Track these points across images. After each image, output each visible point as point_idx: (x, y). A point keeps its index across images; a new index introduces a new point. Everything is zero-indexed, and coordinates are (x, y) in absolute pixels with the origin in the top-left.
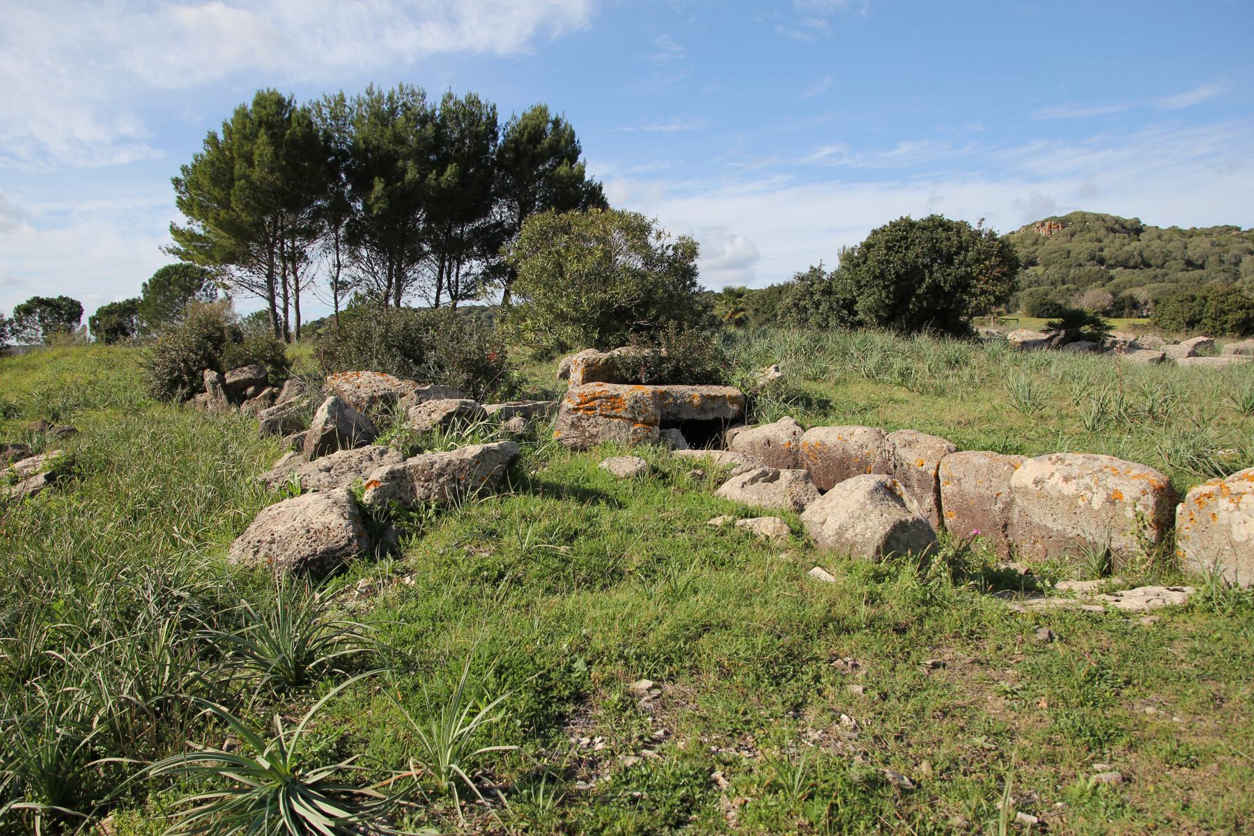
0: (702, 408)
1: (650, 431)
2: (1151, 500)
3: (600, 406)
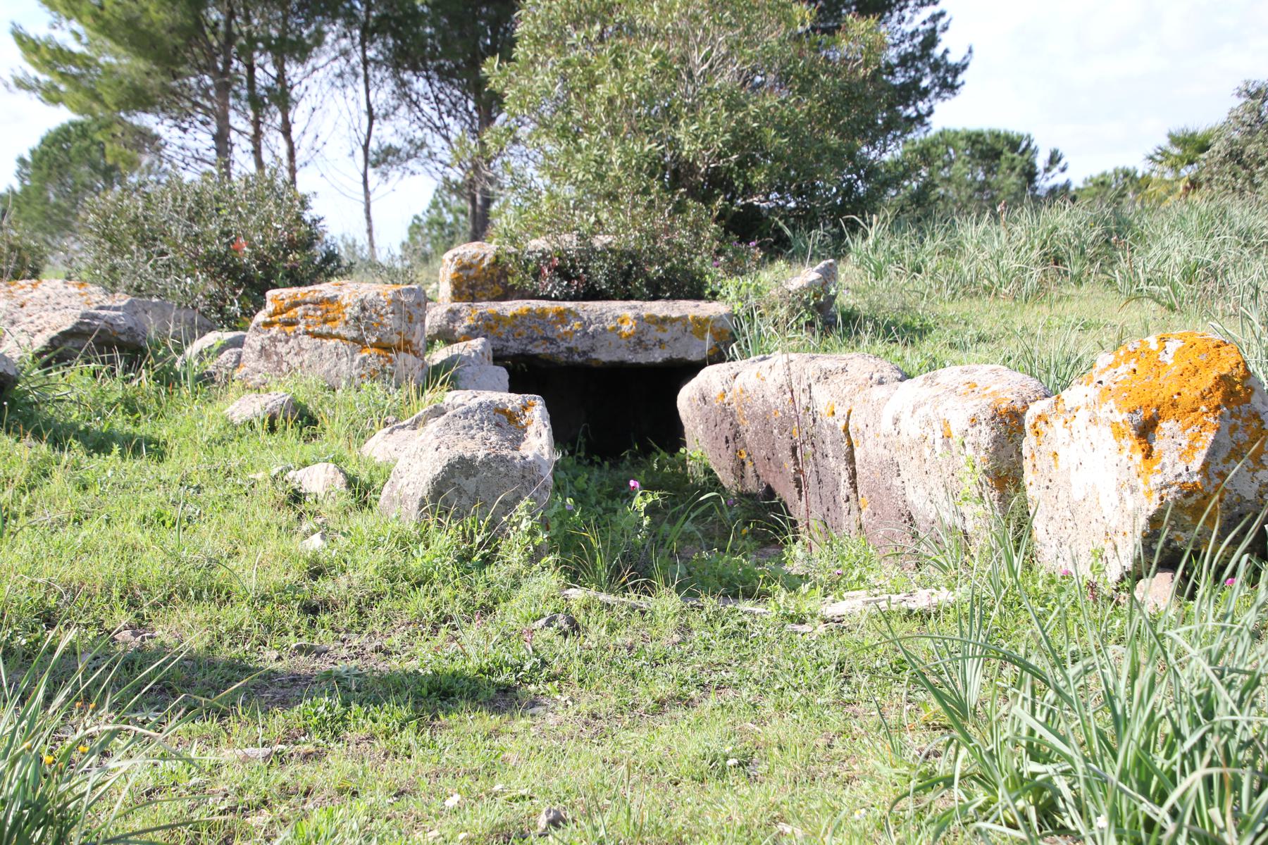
0: (639, 341)
1: (390, 360)
2: (985, 436)
3: (305, 316)
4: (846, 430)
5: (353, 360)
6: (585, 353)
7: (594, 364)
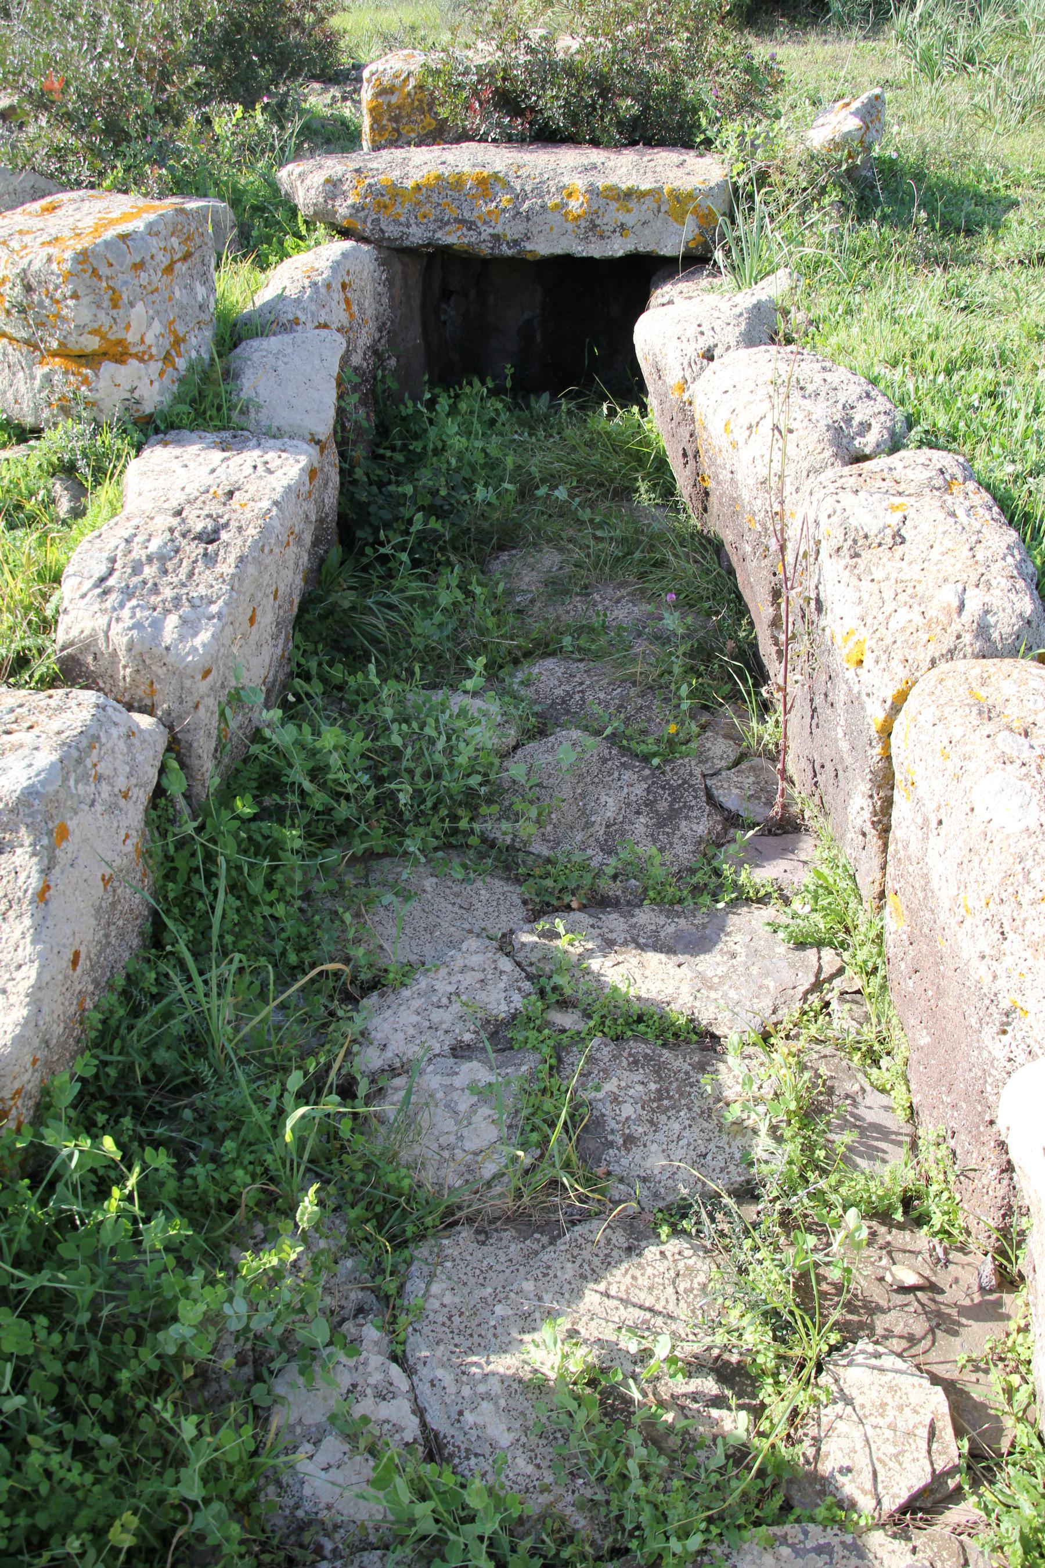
0: (592, 228)
1: (86, 381)
4: (886, 732)
5: (33, 378)
6: (516, 242)
7: (529, 257)
